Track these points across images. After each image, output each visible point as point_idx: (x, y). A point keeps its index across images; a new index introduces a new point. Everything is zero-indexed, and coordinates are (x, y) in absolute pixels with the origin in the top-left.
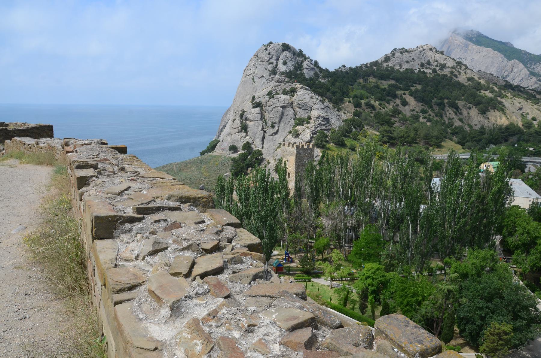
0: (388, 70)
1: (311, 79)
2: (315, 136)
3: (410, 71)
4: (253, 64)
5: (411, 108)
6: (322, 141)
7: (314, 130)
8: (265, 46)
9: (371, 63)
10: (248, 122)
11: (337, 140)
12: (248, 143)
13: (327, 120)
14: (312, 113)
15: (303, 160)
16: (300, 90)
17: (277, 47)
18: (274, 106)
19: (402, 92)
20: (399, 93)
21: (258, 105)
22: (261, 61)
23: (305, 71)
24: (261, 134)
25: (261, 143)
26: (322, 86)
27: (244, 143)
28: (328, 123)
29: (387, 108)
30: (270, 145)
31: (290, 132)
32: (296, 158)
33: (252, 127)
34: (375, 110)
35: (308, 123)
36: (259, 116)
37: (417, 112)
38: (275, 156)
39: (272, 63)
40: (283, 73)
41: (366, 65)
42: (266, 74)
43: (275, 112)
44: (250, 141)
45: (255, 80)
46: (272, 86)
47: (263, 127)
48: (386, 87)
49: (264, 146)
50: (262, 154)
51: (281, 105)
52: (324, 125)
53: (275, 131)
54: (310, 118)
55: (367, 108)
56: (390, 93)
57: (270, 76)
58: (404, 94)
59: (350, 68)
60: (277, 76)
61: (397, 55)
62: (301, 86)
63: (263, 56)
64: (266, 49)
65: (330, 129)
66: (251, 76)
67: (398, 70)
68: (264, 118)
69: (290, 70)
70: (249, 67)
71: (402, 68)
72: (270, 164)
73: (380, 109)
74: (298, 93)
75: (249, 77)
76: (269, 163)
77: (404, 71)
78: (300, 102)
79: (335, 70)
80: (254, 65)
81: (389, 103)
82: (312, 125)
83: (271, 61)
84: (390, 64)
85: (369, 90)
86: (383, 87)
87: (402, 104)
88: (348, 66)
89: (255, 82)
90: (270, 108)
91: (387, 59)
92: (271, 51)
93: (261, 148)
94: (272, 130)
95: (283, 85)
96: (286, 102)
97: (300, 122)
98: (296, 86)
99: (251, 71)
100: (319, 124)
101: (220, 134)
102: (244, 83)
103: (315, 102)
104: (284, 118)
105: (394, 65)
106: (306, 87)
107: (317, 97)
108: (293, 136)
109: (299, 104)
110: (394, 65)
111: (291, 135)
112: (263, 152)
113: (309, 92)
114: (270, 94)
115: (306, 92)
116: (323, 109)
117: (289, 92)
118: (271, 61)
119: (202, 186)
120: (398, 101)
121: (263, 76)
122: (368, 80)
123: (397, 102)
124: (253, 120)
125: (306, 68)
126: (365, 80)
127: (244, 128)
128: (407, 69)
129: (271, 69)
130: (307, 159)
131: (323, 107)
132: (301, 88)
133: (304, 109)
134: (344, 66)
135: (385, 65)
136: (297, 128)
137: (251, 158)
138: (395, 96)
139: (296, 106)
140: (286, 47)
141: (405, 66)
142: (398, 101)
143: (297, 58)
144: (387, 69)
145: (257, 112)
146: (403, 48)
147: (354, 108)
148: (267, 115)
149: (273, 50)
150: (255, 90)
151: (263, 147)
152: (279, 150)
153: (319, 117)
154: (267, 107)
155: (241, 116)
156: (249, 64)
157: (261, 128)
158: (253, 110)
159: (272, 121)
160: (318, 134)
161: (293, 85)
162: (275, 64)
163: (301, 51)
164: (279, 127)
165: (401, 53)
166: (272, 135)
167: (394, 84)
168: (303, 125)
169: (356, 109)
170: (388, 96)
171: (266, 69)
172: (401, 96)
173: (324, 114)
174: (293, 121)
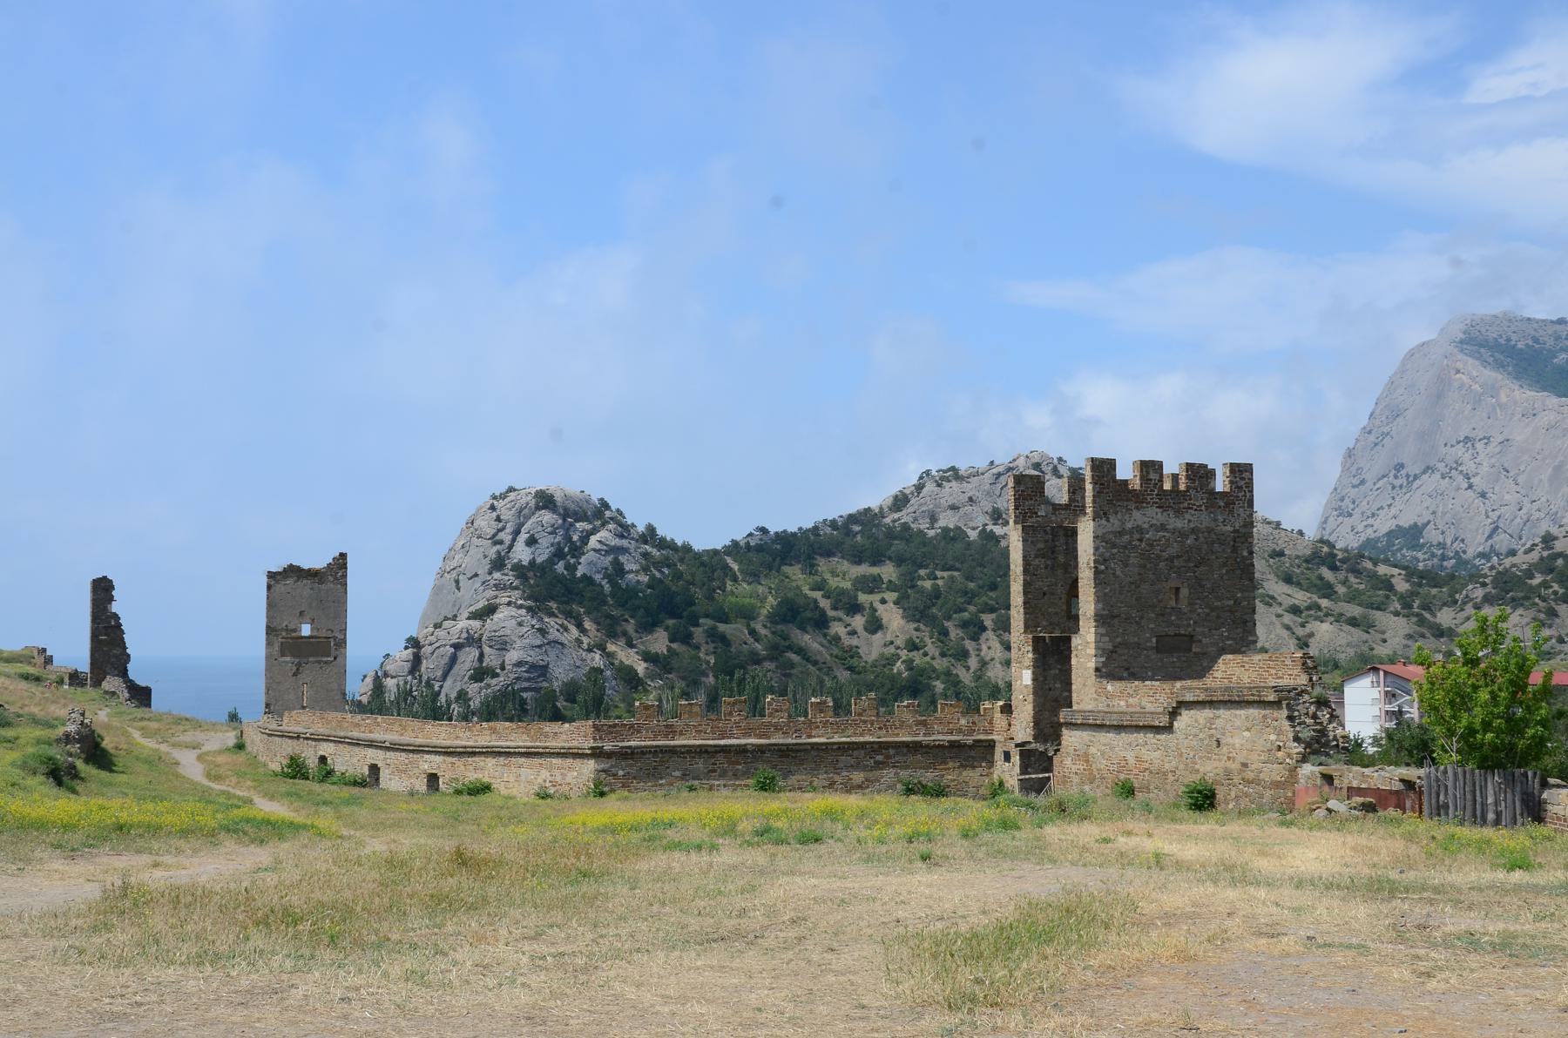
3: (953, 536)
5: (889, 638)
7: (499, 691)
9: (850, 516)
13: (542, 670)
17: (523, 501)
18: (437, 645)
22: (478, 538)
28: (544, 675)
36: (407, 666)
37: (898, 648)
39: (501, 542)
41: (833, 524)
43: (437, 657)
45: (461, 584)
51: (452, 642)
52: (528, 680)
55: (707, 643)
58: (883, 601)
59: (776, 533)
61: (930, 487)
63: (483, 524)
64: (493, 508)
66: (454, 574)
68: (420, 671)
71: (936, 525)
77: (938, 535)
78: (493, 634)
80: (463, 547)
83: (501, 536)
84: (905, 516)
87: (866, 629)
89: (459, 589)
91: (900, 501)
96: (464, 635)
100: (518, 679)
102: (437, 590)
105: (916, 519)
109: (490, 639)
115: (513, 614)
116: (539, 647)
118: (501, 536)
121: (476, 575)
123: (853, 624)
124: (394, 674)
125: (595, 550)
128: (946, 530)
129: (494, 556)
131: (538, 642)
132: (509, 604)
134: (763, 530)
140: (545, 500)
141: (947, 520)
142: (858, 621)
143: (578, 525)
144: (891, 534)
149: (510, 509)
153: (519, 664)
156: (454, 545)
163: (605, 505)
164: (441, 687)
171: (485, 557)
173: (533, 657)
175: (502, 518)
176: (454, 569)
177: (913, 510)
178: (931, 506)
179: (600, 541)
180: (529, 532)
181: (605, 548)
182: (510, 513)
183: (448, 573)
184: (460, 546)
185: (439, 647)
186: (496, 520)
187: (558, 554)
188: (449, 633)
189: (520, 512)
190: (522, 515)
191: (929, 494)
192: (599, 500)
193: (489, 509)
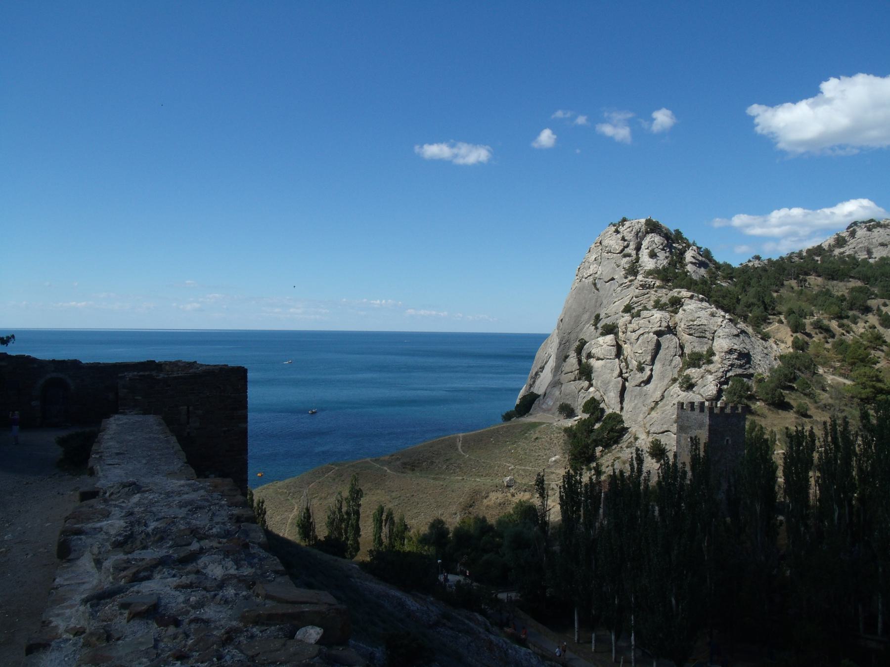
0: (844, 262)
1: (703, 281)
2: (725, 387)
4: (594, 257)
6: (741, 397)
7: (722, 377)
8: (614, 225)
9: (809, 251)
10: (592, 361)
11: (770, 395)
12: (593, 399)
14: (715, 344)
16: (687, 301)
17: (637, 227)
18: (641, 331)
19: (880, 301)
20: (873, 303)
21: (611, 330)
23: (690, 268)
24: (618, 382)
25: (619, 400)
26: (726, 294)
27: (585, 400)
29: (854, 332)
30: (636, 405)
31: (674, 380)
32: (709, 432)
33: (600, 370)
34: (833, 336)
35: (710, 362)
36: (614, 350)
38: (648, 425)
39: (629, 255)
40: (649, 273)
42: (619, 274)
43: (643, 343)
44: (598, 397)
45: (598, 286)
46: (631, 296)
47: (621, 371)
48: (846, 293)
49: (625, 405)
50: (622, 422)
51: (654, 329)
52: (741, 366)
53: (645, 378)
54: (711, 353)
56: (855, 304)
57: (626, 278)
59: (769, 260)
60: (640, 277)
61: (861, 232)
62: (690, 294)
63: (611, 243)
64: (617, 232)
65: (752, 375)
66: (591, 279)
67: (864, 260)
68: (623, 355)
69: (664, 266)
70: (587, 264)
71: (873, 256)
72: (639, 441)
73: (844, 335)
74: (685, 307)
75: (587, 281)
76: (636, 439)
77: (876, 262)
78: (691, 323)
79: (741, 264)
80: (595, 260)
81: (856, 323)
82: (718, 363)
83: (627, 251)
84: (848, 250)
85: (813, 300)
86: (840, 294)
87: (882, 325)
88: (764, 257)
89: (598, 290)
90: (634, 336)
91: (840, 242)
92: (625, 233)
93: (619, 409)
94: (639, 375)
95: (653, 292)
96: (664, 324)
97: (696, 360)
98: (681, 294)
99: (591, 269)
100: (732, 365)
101: (534, 382)
103: (719, 323)
104: (662, 352)
105: (856, 252)
106: (701, 296)
107: (723, 313)
108: (681, 387)
109: (689, 327)
110: (856, 252)
111: (677, 385)
112: (624, 418)
113: (705, 304)
114: (628, 309)
115: (700, 306)
116: (737, 335)
117: (667, 305)
118: (627, 251)
119: (510, 480)
120: (873, 319)
121: (613, 279)
122: (806, 281)
125: (691, 263)
126: (801, 281)
127: (586, 372)
128: (882, 259)
129: (627, 266)
131: (735, 332)
132: (691, 297)
133: (699, 337)
134: (758, 258)
135: (837, 252)
136: (688, 372)
137: (601, 428)
138: (867, 310)
139: (684, 331)
140: (653, 227)
142: (873, 319)
145: (610, 343)
146: (872, 220)
147: (790, 333)
148: (627, 349)
149: (630, 232)
150: (598, 304)
151: (622, 409)
152: (653, 414)
153: (731, 351)
154: (629, 333)
155: (579, 350)
157: (617, 372)
158: (601, 340)
159: (638, 359)
160: (730, 383)
161: (675, 293)
162: (634, 256)
163: (678, 233)
164: (652, 370)
165: (869, 230)
166: (639, 385)
167: (861, 287)
168: (700, 367)
169: (795, 335)
170: (851, 309)
172: (879, 309)
174: (678, 358)
175: (626, 238)
176: (591, 275)
177: (853, 247)
178: (866, 244)
179: (693, 257)
180: (648, 248)
181: (697, 261)
182: (630, 235)
183: (586, 278)
184: (593, 259)
185: (643, 334)
186: (621, 240)
187: (672, 264)
188: (649, 322)
189: (637, 235)
190: (639, 237)
191: (864, 236)
192: (675, 231)
193: (614, 232)
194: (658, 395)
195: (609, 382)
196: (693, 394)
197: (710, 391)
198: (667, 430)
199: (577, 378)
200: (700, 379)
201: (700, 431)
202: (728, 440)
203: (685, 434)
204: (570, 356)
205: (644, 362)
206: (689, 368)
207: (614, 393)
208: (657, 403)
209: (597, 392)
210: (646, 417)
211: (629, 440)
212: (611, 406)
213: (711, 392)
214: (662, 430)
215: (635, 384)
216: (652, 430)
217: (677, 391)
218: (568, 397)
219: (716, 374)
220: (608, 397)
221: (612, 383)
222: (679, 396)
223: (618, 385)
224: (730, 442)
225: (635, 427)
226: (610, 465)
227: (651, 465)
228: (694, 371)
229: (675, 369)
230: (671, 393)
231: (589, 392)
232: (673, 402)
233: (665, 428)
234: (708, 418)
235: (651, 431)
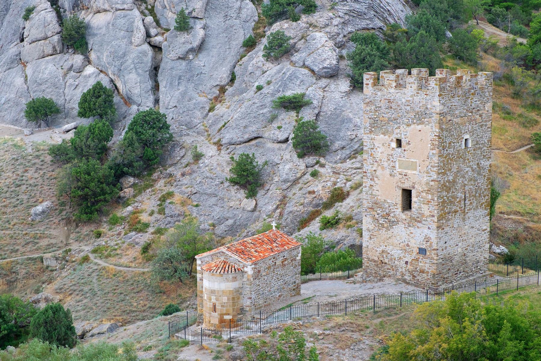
15: (460, 137)
30: (184, 94)
50: (166, 127)
53: (196, 44)
76: (198, 157)
130: (472, 133)
152: (221, 109)
157: (140, 34)
168: (296, 19)
194: (223, 75)
195: (124, 55)
196: (293, 68)
197: (325, 60)
198: (256, 135)
199: (58, 50)
200: (300, 40)
201: (420, 127)
202: (466, 140)
203: (384, 134)
204: (38, 8)
205: (190, 13)
206: (275, 21)
207: (138, 74)
208: (223, 90)
209: (102, 75)
210: (207, 115)
211: (185, 161)
212: (135, 98)
213: (328, 62)
214: (246, 137)
215: (177, 56)
216: (228, 136)
217: (260, 64)
218: (43, 87)
219: (328, 29)
220: (125, 83)
221: (132, 56)
222: (264, 72)
223: (145, 59)
224: (470, 145)
225: (188, 135)
226: (156, 209)
227: (238, 203)
228: (286, 25)
229: (248, 24)
230: (250, 68)
231: (85, 77)
232: (256, 84)
233: (252, 131)
234: (437, 99)
235: (224, 141)
